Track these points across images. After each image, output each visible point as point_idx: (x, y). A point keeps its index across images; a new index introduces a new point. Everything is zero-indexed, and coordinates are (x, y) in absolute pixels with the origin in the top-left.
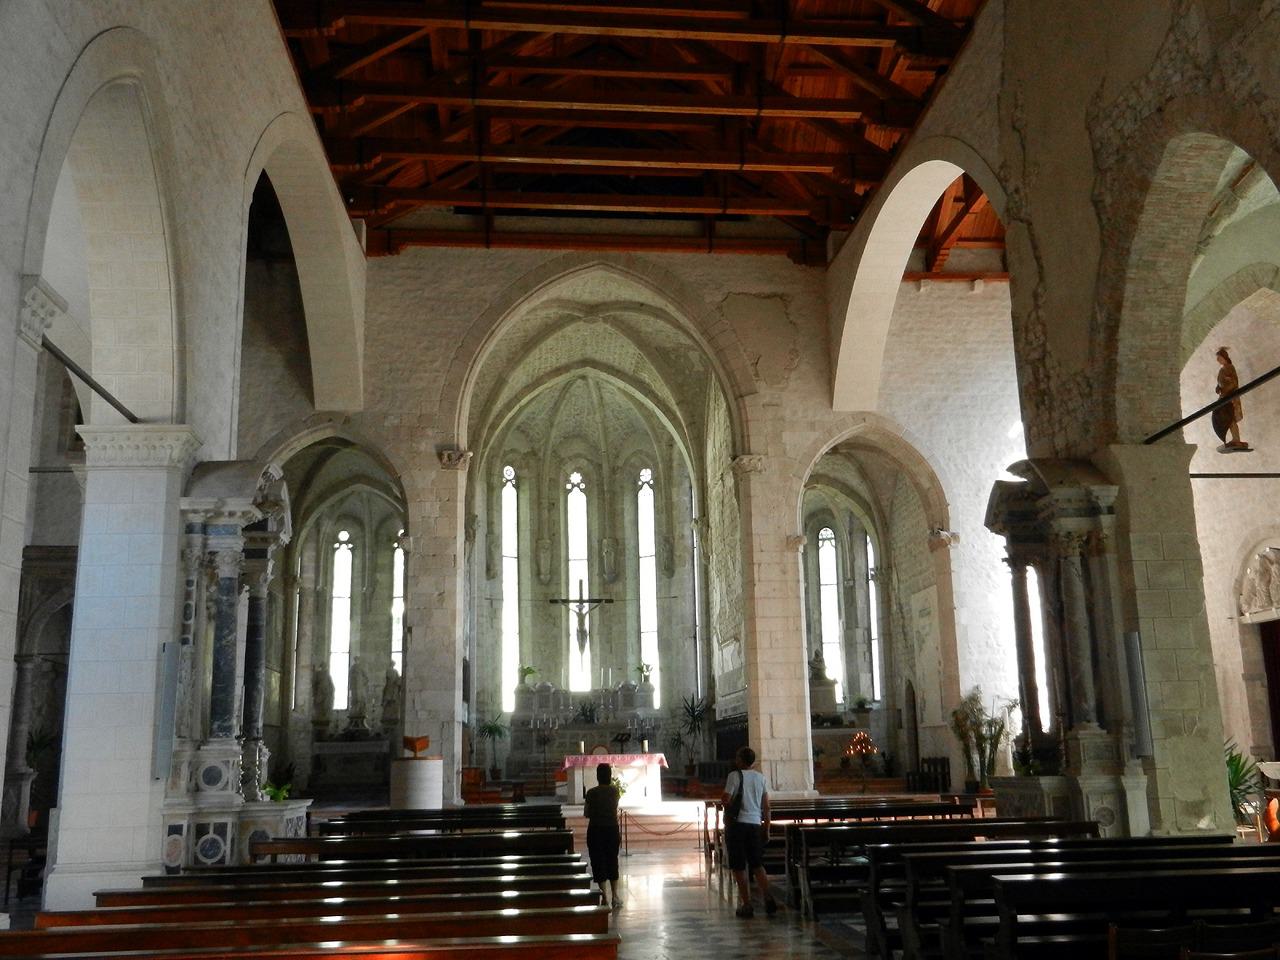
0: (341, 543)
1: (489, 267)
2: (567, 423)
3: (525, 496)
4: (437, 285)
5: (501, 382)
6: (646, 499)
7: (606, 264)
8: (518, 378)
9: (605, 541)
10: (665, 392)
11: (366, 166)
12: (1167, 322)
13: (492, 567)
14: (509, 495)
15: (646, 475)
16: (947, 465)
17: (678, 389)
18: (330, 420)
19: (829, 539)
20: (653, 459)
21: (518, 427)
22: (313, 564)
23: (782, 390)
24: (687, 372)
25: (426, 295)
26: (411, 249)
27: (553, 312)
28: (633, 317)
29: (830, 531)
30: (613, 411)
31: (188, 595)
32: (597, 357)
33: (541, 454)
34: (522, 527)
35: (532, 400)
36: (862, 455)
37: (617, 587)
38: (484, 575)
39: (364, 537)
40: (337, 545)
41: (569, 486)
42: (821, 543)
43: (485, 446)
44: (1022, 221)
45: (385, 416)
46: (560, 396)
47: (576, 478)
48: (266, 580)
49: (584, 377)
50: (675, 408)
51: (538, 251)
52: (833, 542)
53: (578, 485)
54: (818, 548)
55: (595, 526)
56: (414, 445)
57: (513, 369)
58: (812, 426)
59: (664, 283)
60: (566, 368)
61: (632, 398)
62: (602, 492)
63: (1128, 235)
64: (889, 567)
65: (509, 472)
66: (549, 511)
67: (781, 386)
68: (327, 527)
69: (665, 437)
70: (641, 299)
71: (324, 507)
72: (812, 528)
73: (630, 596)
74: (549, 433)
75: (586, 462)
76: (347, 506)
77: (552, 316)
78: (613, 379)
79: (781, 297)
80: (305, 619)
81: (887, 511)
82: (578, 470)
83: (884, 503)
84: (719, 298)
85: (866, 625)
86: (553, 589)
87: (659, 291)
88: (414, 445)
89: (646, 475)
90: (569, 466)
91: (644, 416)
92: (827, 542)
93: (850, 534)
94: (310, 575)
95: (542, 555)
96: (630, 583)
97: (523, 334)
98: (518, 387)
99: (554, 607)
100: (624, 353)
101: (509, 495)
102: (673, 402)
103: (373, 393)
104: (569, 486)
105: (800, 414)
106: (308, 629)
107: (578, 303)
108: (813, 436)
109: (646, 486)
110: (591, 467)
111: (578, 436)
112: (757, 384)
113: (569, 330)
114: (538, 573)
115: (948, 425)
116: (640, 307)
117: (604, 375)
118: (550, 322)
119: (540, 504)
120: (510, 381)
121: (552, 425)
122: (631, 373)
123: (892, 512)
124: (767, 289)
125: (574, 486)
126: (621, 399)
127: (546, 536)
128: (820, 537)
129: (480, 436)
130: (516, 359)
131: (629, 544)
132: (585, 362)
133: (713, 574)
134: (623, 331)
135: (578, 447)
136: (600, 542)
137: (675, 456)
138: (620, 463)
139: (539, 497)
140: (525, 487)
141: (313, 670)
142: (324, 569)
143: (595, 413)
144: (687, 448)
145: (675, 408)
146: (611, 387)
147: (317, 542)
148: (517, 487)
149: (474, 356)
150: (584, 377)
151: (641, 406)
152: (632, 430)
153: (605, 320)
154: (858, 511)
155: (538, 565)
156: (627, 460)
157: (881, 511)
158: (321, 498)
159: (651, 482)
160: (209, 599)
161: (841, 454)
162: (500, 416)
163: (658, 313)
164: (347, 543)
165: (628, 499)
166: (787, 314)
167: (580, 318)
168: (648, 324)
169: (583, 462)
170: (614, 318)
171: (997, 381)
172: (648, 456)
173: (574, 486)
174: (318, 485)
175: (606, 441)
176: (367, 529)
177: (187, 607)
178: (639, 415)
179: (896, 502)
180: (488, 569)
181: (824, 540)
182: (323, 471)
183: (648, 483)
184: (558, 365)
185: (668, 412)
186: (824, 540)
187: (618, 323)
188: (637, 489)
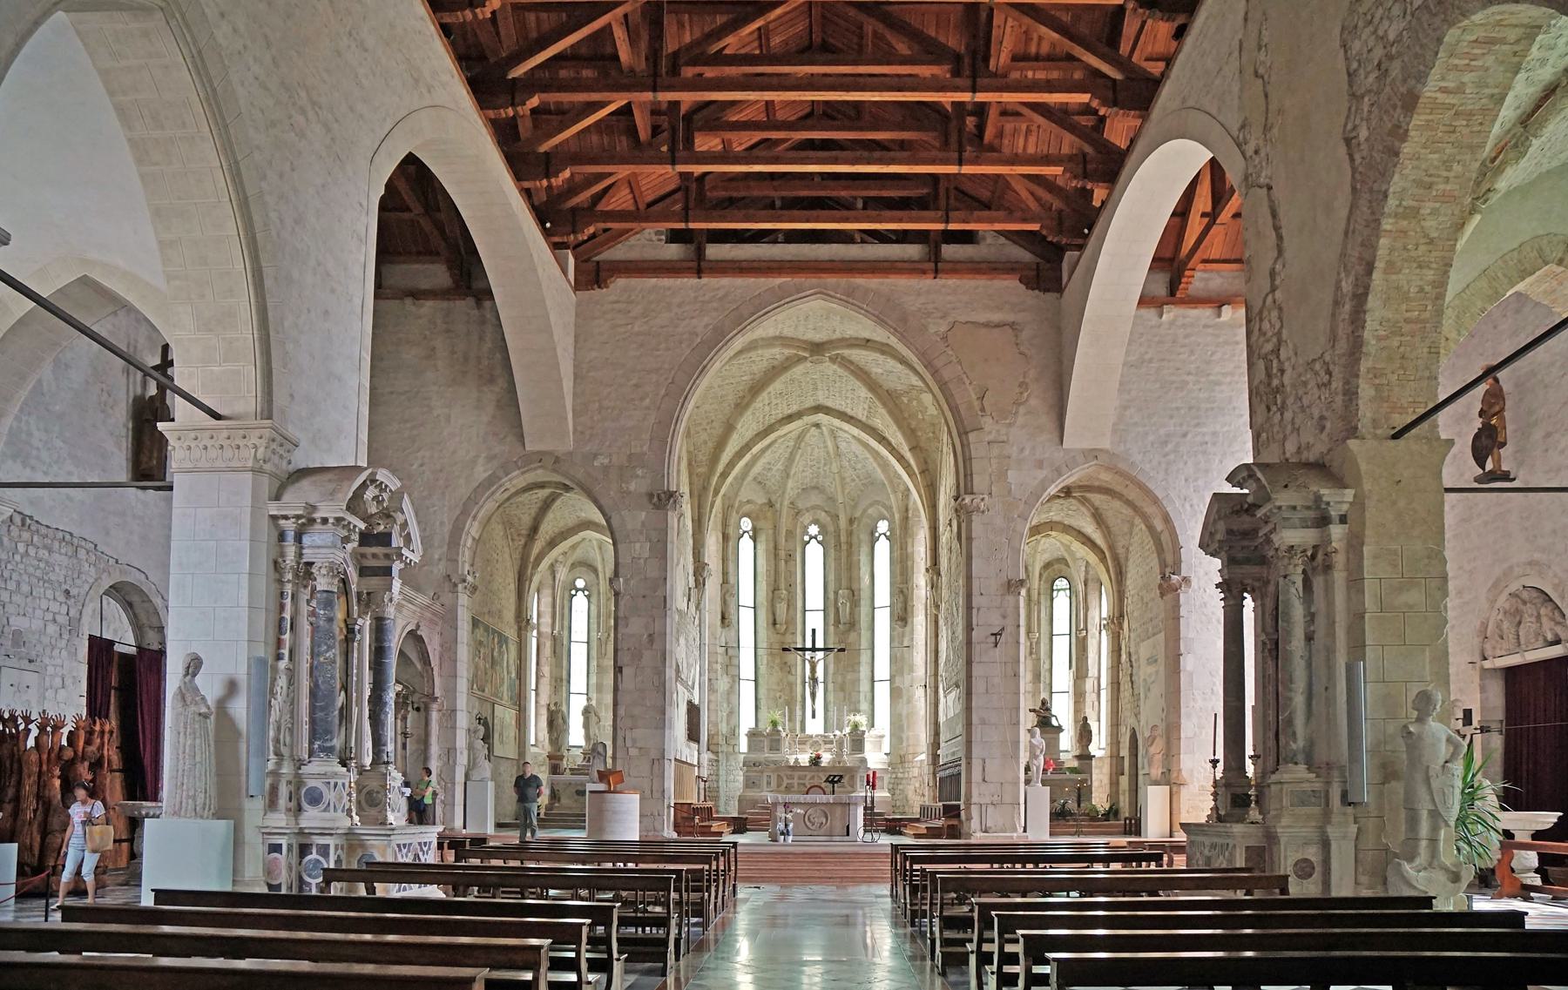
0: (577, 590)
1: (701, 299)
2: (804, 474)
3: (761, 547)
5: (729, 428)
6: (883, 549)
7: (824, 293)
8: (747, 426)
9: (840, 591)
10: (897, 439)
11: (553, 180)
12: (1428, 288)
13: (726, 616)
14: (746, 545)
15: (883, 526)
16: (1183, 505)
17: (910, 433)
19: (1064, 590)
20: (889, 508)
21: (755, 479)
22: (550, 610)
23: (1010, 425)
24: (920, 416)
25: (636, 329)
27: (778, 353)
28: (858, 355)
29: (1066, 581)
30: (849, 461)
31: (282, 607)
32: (829, 403)
33: (778, 506)
34: (759, 578)
35: (769, 446)
36: (1097, 498)
37: (852, 636)
38: (719, 623)
39: (598, 584)
40: (573, 592)
41: (806, 538)
42: (1055, 593)
43: (716, 492)
44: (1261, 187)
45: (595, 456)
46: (795, 446)
47: (814, 530)
48: (391, 600)
49: (817, 425)
50: (908, 456)
52: (1068, 592)
53: (815, 538)
54: (1052, 599)
55: (832, 577)
57: (741, 414)
58: (1040, 464)
59: (887, 313)
60: (799, 415)
61: (866, 446)
62: (838, 545)
63: (1385, 175)
64: (1121, 616)
65: (746, 524)
66: (786, 562)
67: (1008, 421)
68: (562, 574)
69: (902, 488)
70: (866, 335)
71: (555, 553)
72: (1047, 578)
73: (864, 644)
74: (785, 485)
75: (823, 514)
76: (578, 554)
77: (778, 356)
78: (846, 426)
79: (1012, 325)
80: (543, 660)
81: (1122, 557)
82: (816, 522)
83: (1121, 551)
84: (943, 328)
85: (1096, 675)
86: (789, 638)
87: (881, 321)
89: (883, 526)
90: (806, 518)
91: (879, 465)
92: (1061, 592)
93: (1085, 585)
94: (547, 620)
95: (778, 605)
96: (865, 634)
98: (749, 435)
99: (790, 656)
100: (857, 399)
101: (746, 545)
102: (906, 448)
104: (806, 538)
105: (1027, 452)
106: (546, 670)
107: (805, 342)
108: (1041, 474)
109: (883, 537)
110: (829, 519)
111: (815, 487)
112: (984, 419)
113: (798, 370)
114: (775, 623)
115: (1186, 463)
116: (867, 344)
117: (837, 422)
118: (776, 363)
119: (776, 555)
120: (739, 426)
121: (788, 476)
122: (864, 419)
123: (1127, 559)
124: (996, 317)
125: (811, 538)
126: (857, 448)
127: (782, 586)
128: (1055, 588)
129: (709, 483)
130: (743, 404)
131: (865, 595)
132: (819, 409)
133: (941, 622)
134: (852, 372)
135: (815, 499)
136: (836, 593)
137: (911, 505)
138: (857, 514)
139: (776, 548)
140: (762, 538)
141: (548, 709)
142: (562, 614)
143: (831, 464)
144: (920, 496)
145: (908, 456)
146: (846, 435)
147: (554, 588)
148: (754, 539)
150: (817, 425)
151: (876, 454)
152: (870, 482)
153: (833, 360)
154: (1092, 558)
155: (774, 614)
156: (865, 511)
157: (1116, 558)
158: (552, 544)
159: (888, 534)
160: (313, 614)
161: (1074, 497)
162: (731, 465)
163: (884, 349)
164: (583, 590)
165: (865, 549)
166: (1017, 344)
167: (806, 358)
168: (879, 365)
169: (822, 516)
170: (843, 358)
172: (884, 506)
173: (811, 538)
174: (548, 528)
175: (843, 492)
176: (601, 575)
177: (282, 620)
178: (875, 465)
179: (1131, 549)
180: (723, 618)
181: (1058, 590)
182: (550, 515)
183: (885, 534)
184: (789, 412)
185: (901, 459)
186: (1058, 590)
187: (846, 363)
188: (873, 541)
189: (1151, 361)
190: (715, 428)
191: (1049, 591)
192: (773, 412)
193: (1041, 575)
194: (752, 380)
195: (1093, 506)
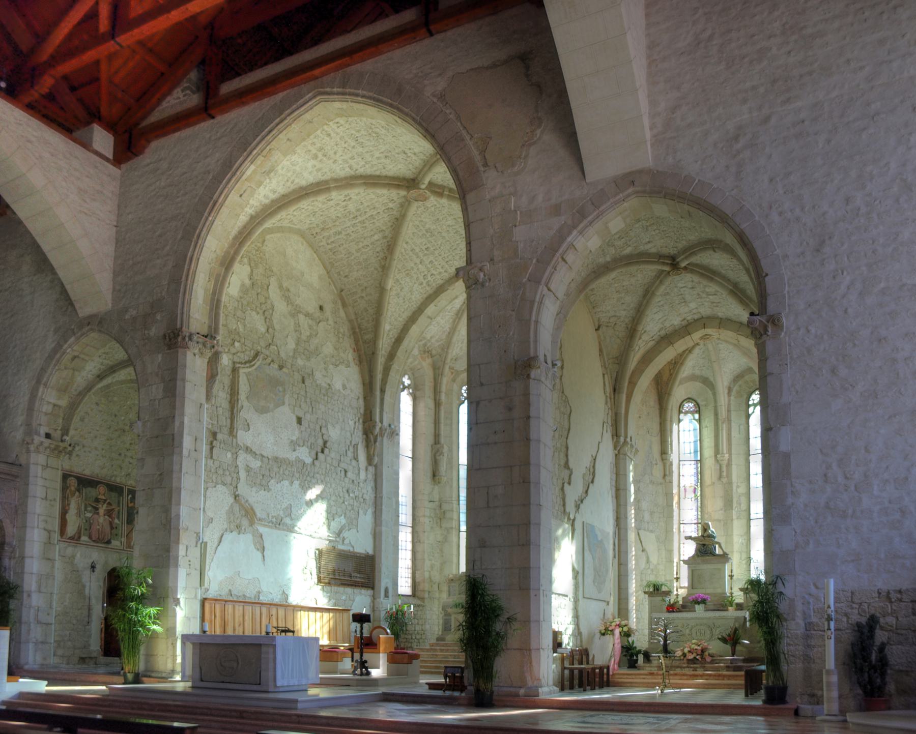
4: (171, 172)
18: (89, 324)
25: (163, 184)
26: (154, 144)
51: (257, 103)
56: (146, 332)
77: (391, 205)
88: (146, 332)
97: (380, 235)
103: (120, 290)
128: (751, 403)
149: (198, 231)
171: (861, 68)
189: (711, 38)
190: (371, 294)
191: (744, 406)
192: (434, 272)
193: (730, 390)
194: (385, 237)
195: (729, 281)
